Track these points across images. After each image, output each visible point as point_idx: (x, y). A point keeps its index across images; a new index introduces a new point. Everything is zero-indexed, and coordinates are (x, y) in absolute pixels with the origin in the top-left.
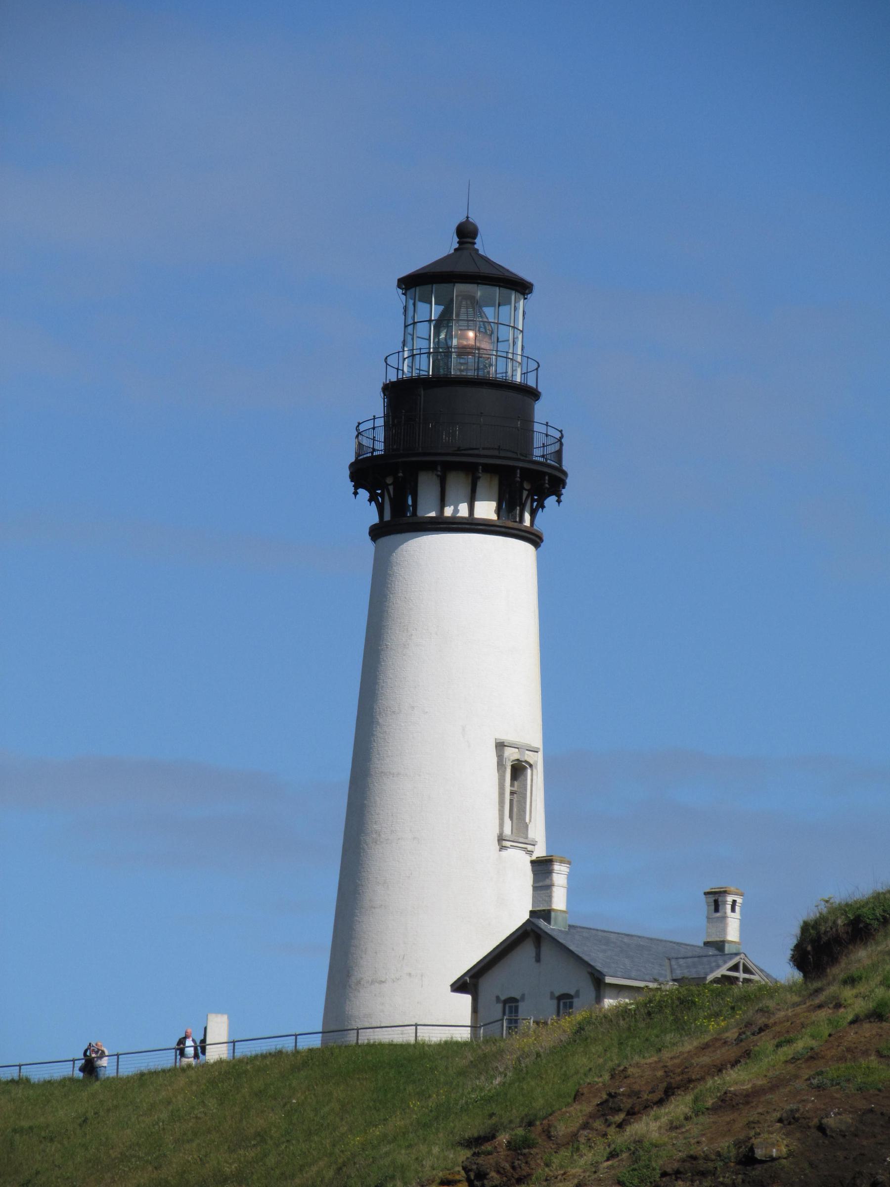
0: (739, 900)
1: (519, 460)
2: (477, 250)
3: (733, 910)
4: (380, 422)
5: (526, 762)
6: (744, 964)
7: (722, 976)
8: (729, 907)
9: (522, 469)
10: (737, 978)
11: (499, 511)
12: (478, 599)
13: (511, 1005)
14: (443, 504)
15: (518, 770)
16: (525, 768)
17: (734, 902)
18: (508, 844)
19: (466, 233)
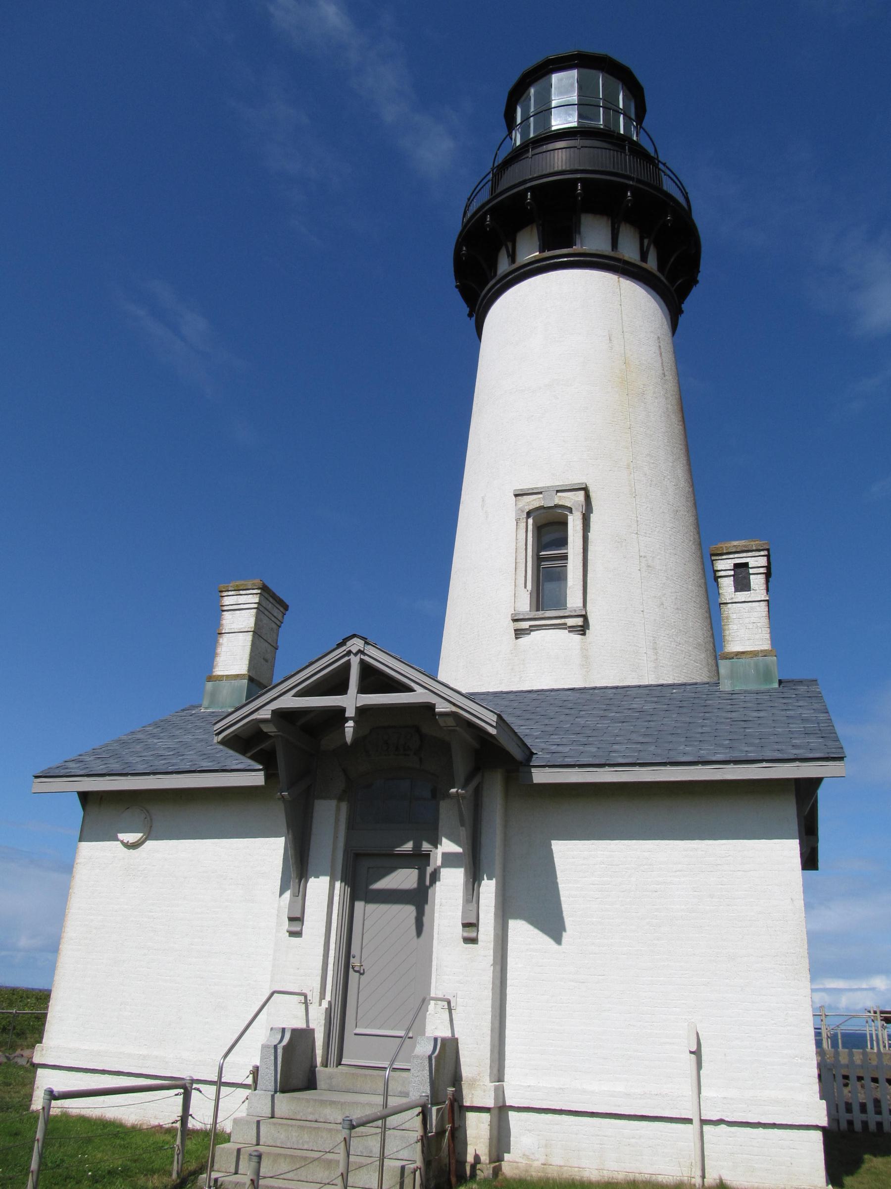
3: (742, 584)
5: (557, 506)
8: (727, 585)
10: (338, 714)
16: (567, 516)
17: (741, 569)
18: (525, 625)
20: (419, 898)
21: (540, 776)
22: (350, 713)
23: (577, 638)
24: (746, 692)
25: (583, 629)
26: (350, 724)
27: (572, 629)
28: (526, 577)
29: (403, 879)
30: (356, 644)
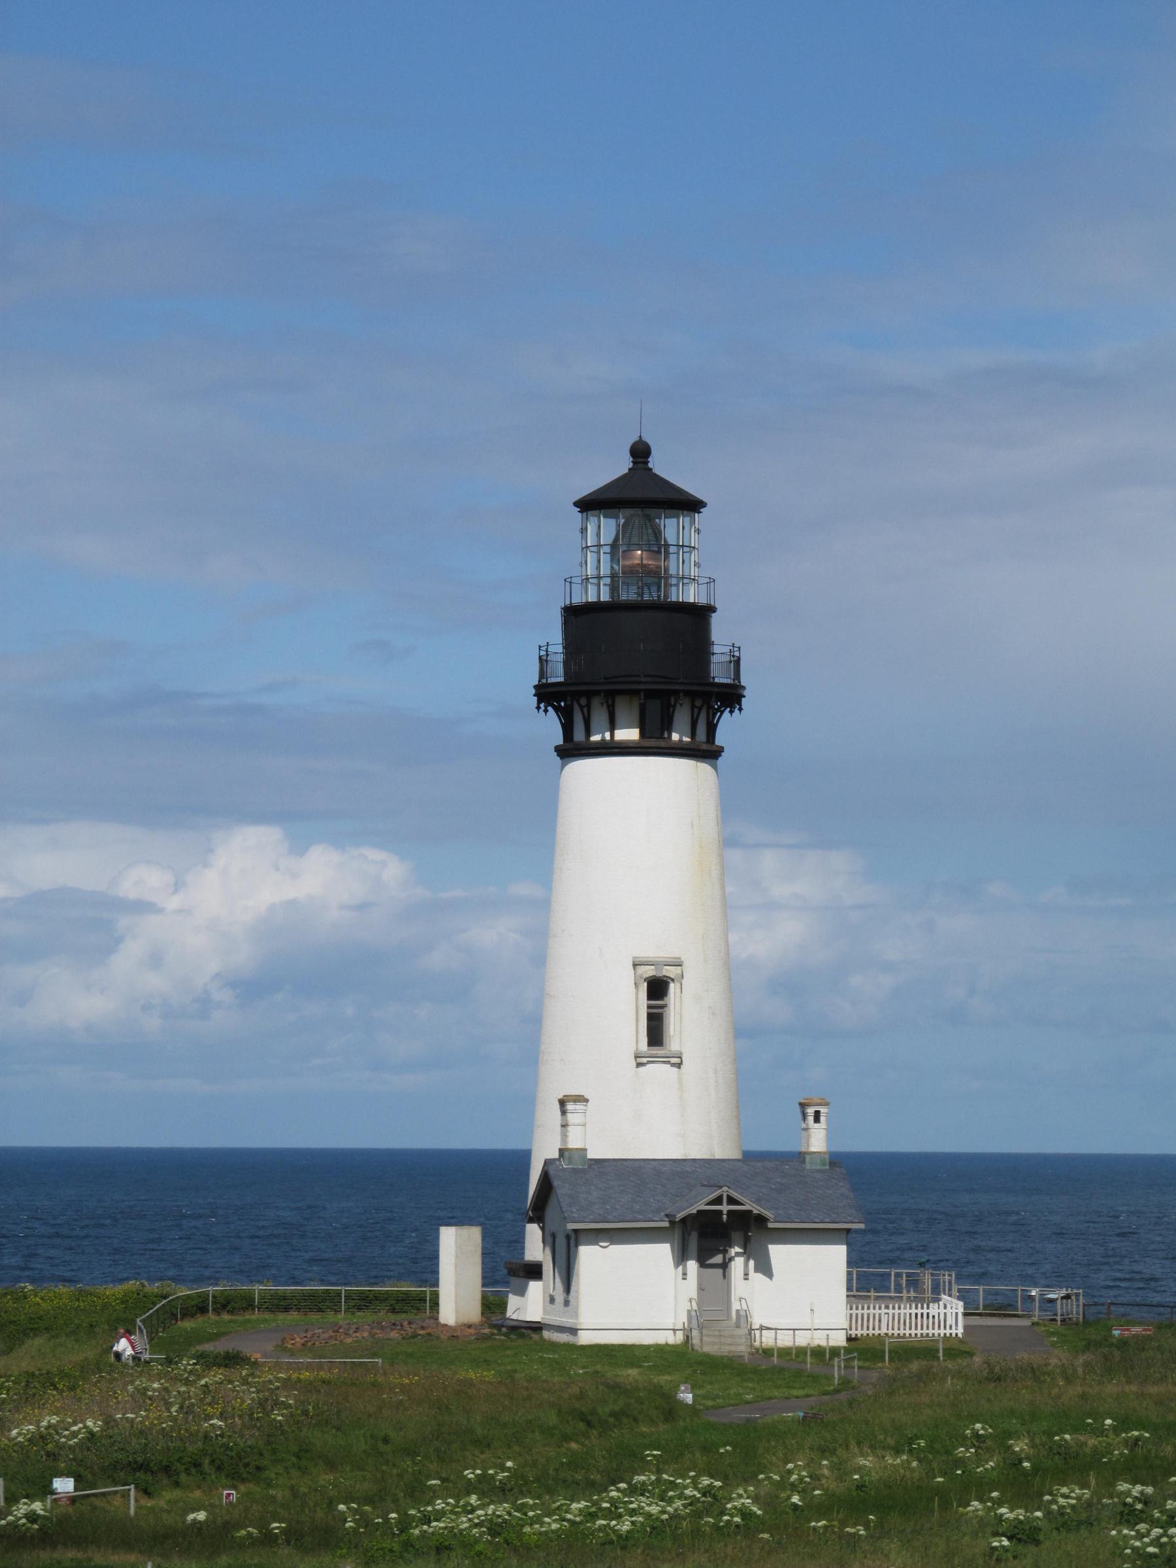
0: (823, 1110)
1: (639, 683)
3: (817, 1118)
4: (560, 649)
6: (728, 1196)
7: (701, 1213)
8: (811, 1119)
9: (645, 691)
10: (720, 1212)
11: (642, 734)
12: (636, 818)
13: (554, 1236)
14: (588, 733)
15: (657, 988)
18: (644, 1060)
19: (640, 452)
20: (725, 1266)
21: (770, 1225)
23: (675, 1069)
24: (818, 1171)
25: (679, 1066)
27: (673, 1065)
28: (637, 1020)
29: (718, 1259)
30: (725, 1189)
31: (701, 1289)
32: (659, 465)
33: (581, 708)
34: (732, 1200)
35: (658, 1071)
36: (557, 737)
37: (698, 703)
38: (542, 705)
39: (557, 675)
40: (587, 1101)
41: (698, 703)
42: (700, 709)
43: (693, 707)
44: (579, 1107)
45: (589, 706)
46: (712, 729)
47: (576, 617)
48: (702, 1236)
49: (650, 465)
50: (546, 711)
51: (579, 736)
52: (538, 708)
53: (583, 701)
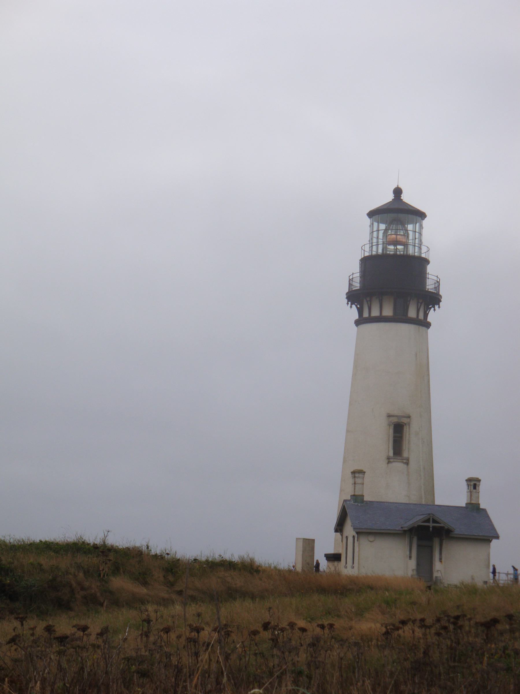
2: (402, 200)
6: (433, 519)
10: (429, 527)
13: (347, 537)
18: (392, 460)
19: (398, 192)
22: (431, 527)
25: (407, 464)
26: (431, 529)
31: (418, 565)
32: (406, 198)
33: (367, 301)
34: (434, 521)
35: (398, 465)
36: (356, 317)
37: (421, 301)
38: (350, 303)
39: (357, 285)
40: (365, 472)
41: (421, 301)
42: (421, 304)
43: (418, 303)
44: (361, 475)
45: (371, 301)
46: (426, 315)
47: (366, 262)
48: (419, 539)
49: (402, 198)
50: (351, 307)
51: (366, 315)
52: (348, 304)
53: (368, 299)
